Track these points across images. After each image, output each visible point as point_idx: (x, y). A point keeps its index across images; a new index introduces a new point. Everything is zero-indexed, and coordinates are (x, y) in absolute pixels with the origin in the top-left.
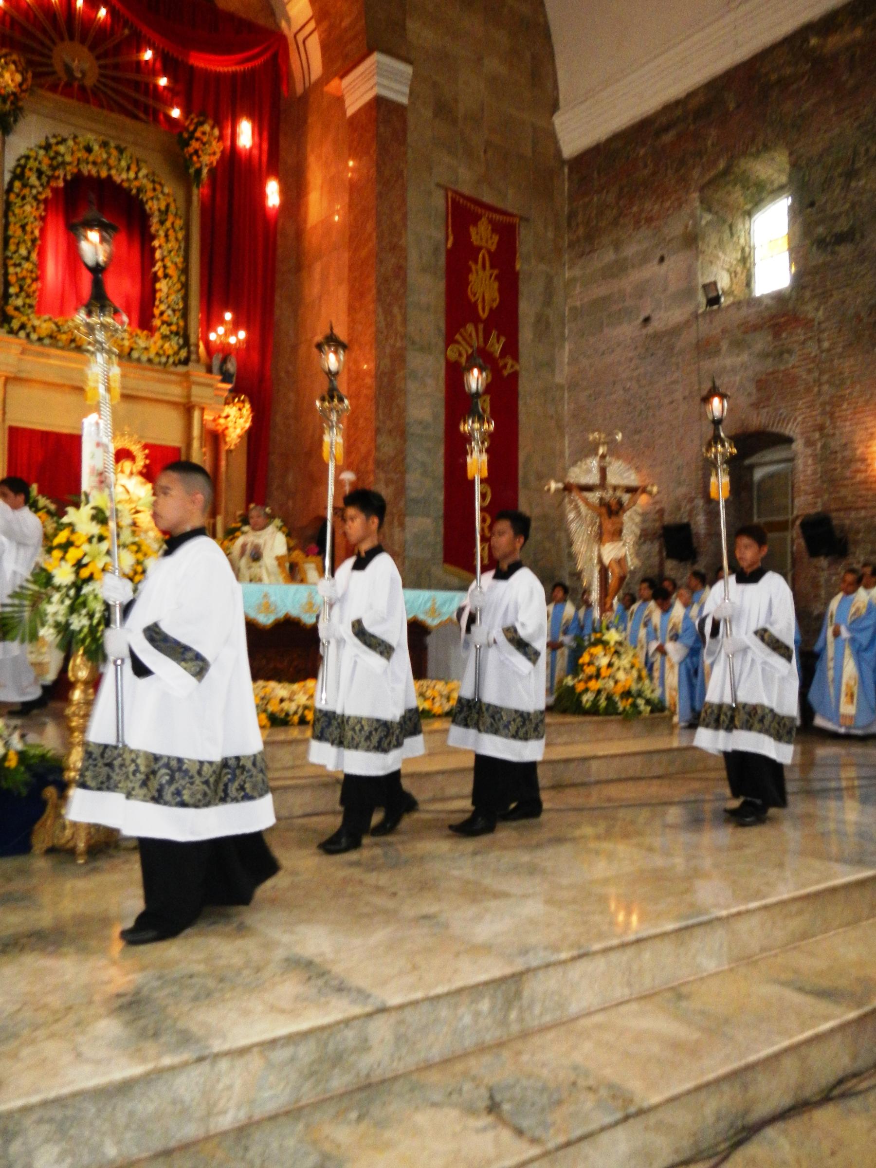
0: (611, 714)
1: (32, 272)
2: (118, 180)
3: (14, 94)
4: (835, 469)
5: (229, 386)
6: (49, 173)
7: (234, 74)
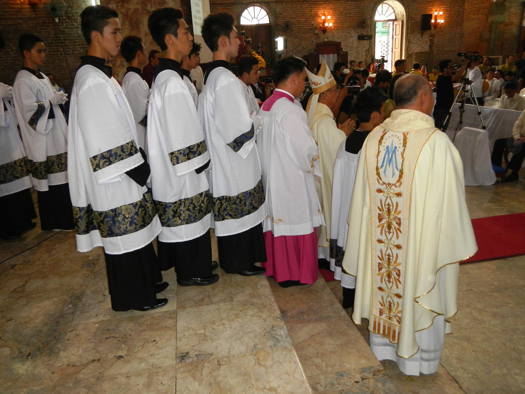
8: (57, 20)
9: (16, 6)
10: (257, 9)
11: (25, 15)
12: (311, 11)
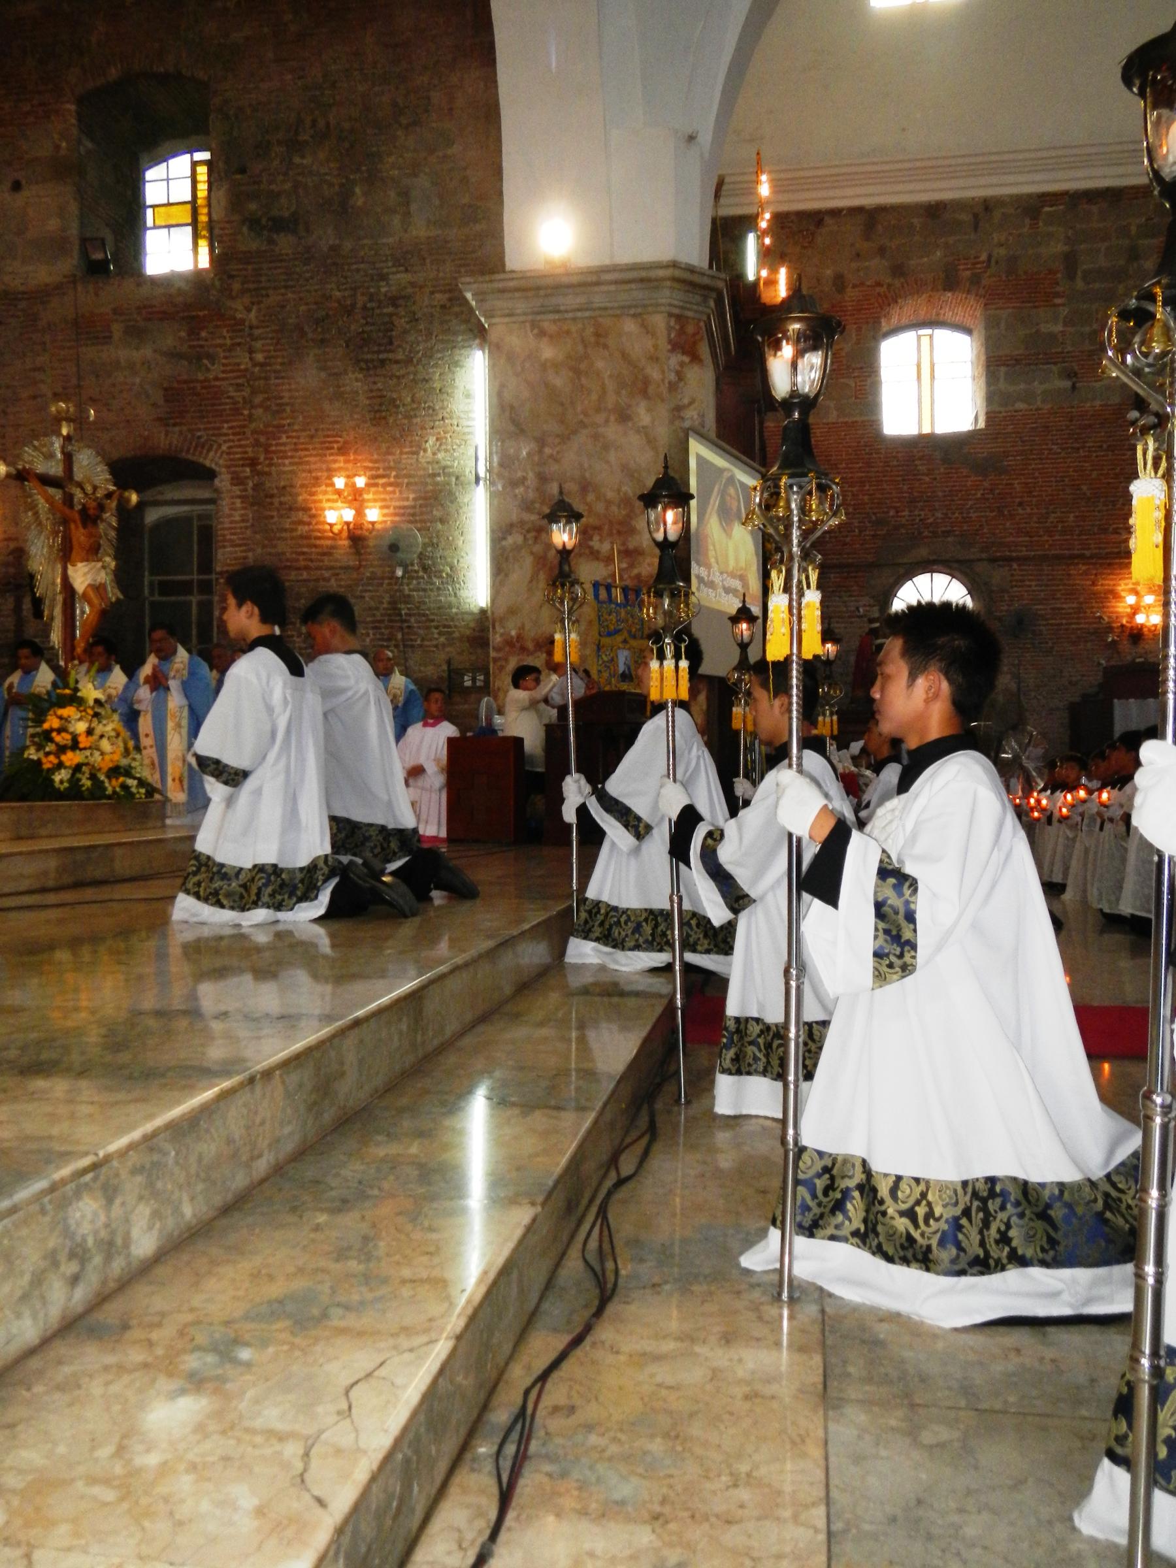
0: (99, 799)
4: (272, 517)
8: (399, 573)
9: (322, 542)
10: (941, 579)
11: (336, 561)
12: (1094, 584)
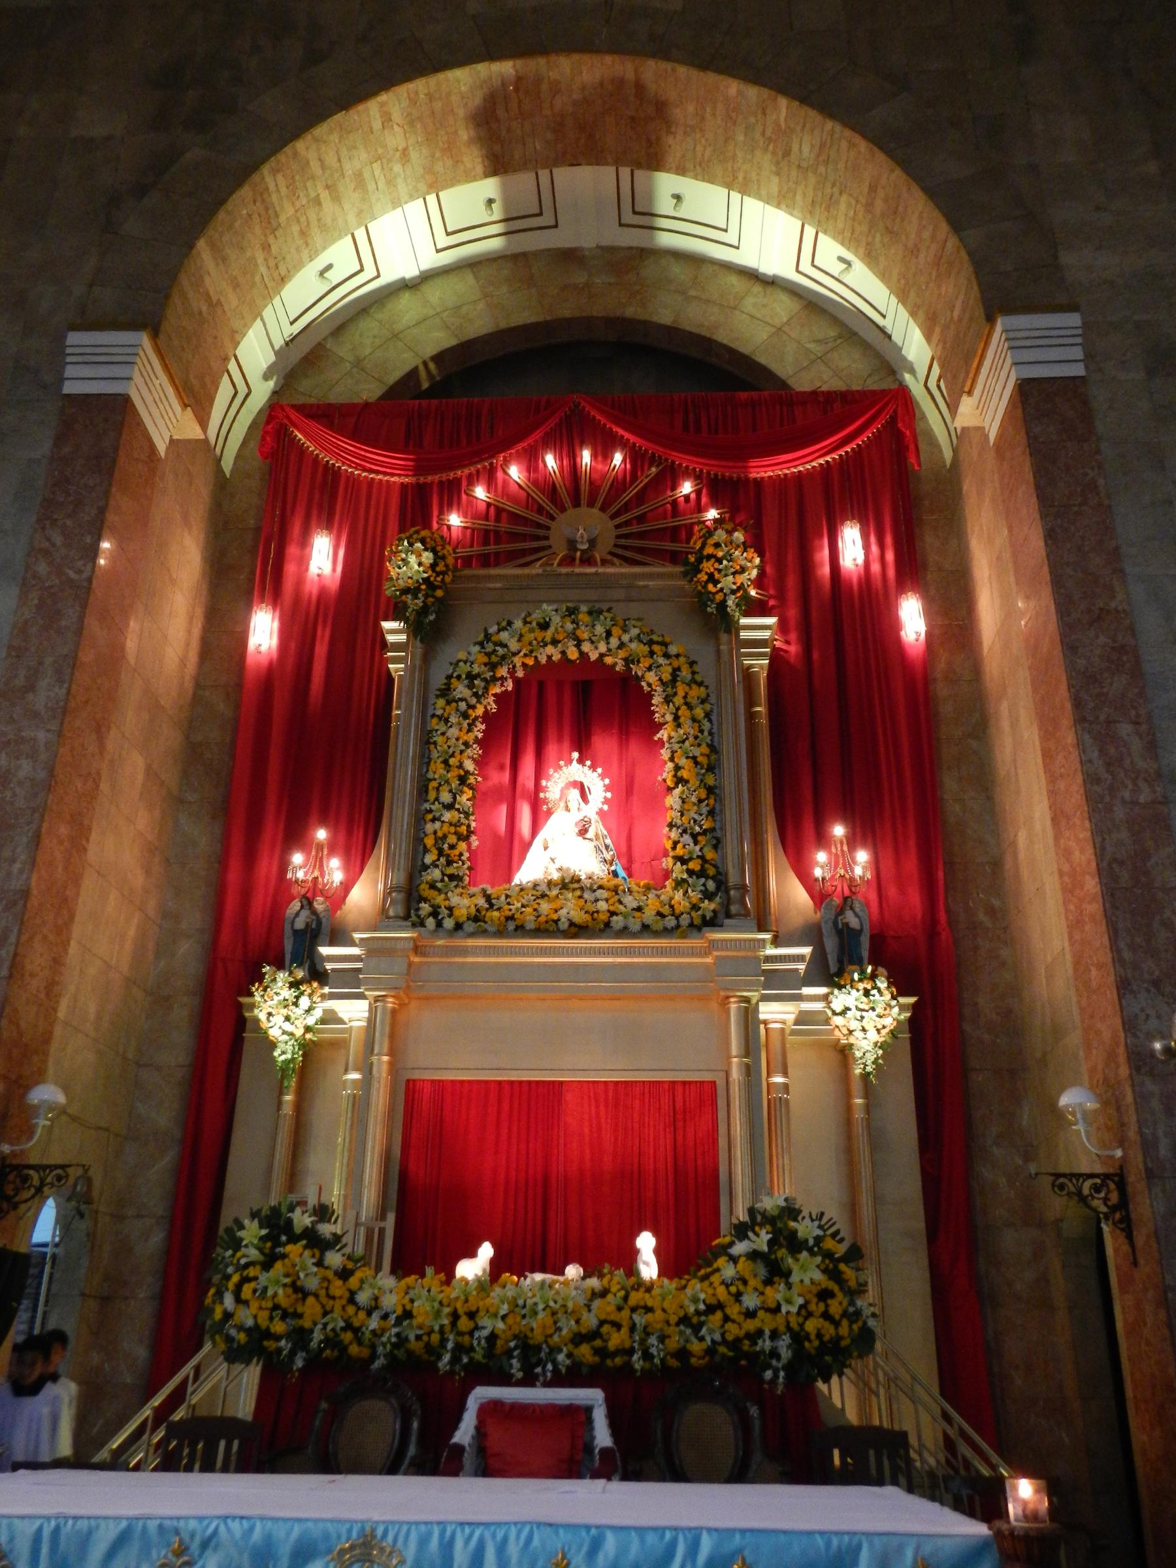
1: (458, 824)
2: (594, 656)
3: (426, 580)
5: (806, 951)
6: (489, 675)
7: (827, 468)
